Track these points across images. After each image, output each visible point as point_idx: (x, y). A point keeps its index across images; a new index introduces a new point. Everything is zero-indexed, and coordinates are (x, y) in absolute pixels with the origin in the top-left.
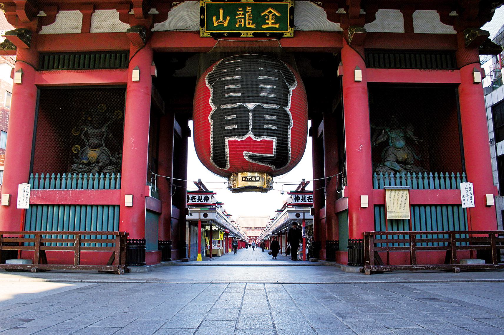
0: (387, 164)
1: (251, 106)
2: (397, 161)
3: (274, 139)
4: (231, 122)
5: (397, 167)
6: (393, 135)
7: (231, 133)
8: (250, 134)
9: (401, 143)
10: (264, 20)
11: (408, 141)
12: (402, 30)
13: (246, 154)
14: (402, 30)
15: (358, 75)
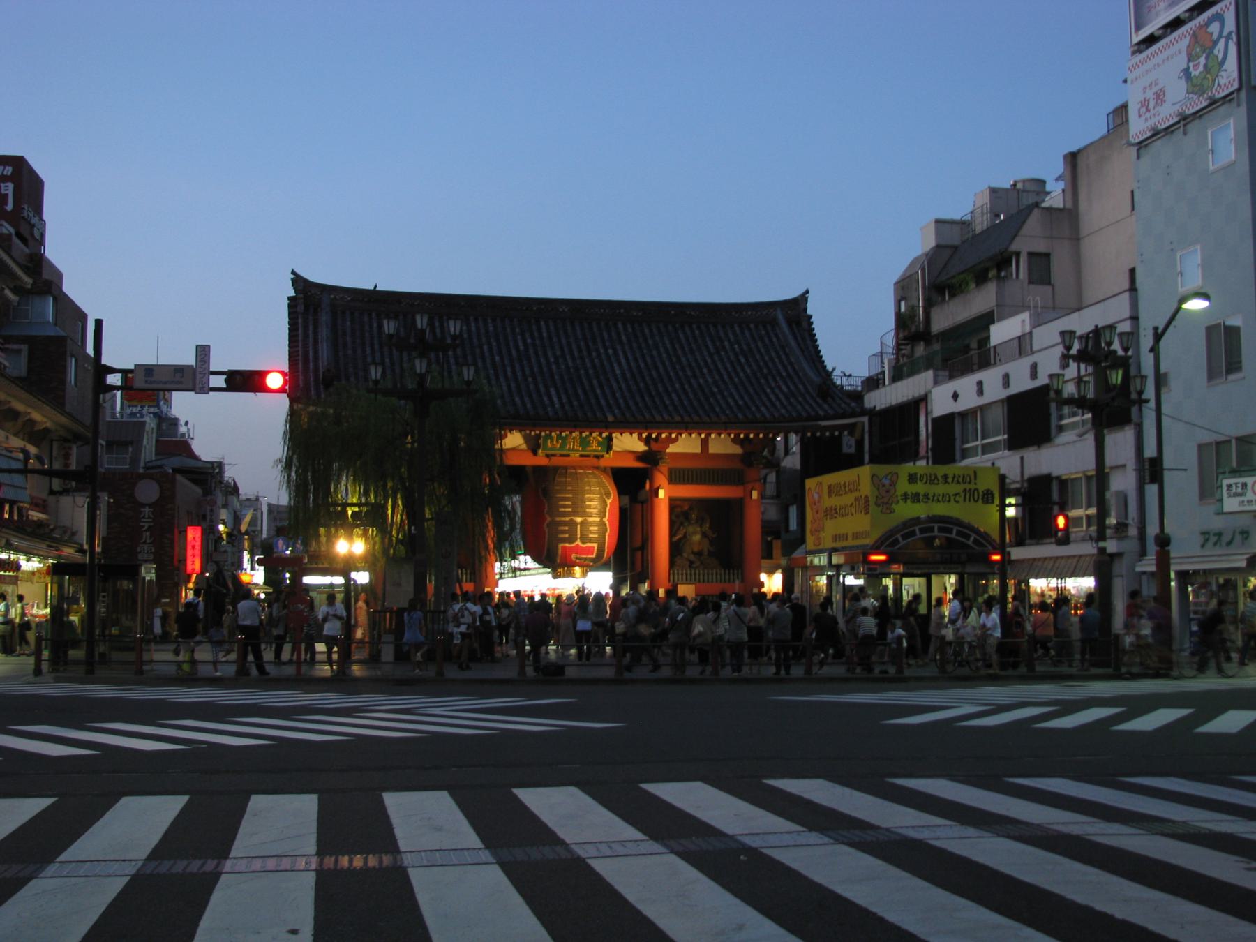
0: (685, 555)
1: (579, 520)
2: (693, 553)
3: (595, 545)
4: (564, 532)
5: (692, 557)
6: (691, 529)
7: (564, 540)
8: (578, 542)
9: (697, 538)
10: (588, 444)
11: (704, 535)
12: (698, 450)
13: (573, 556)
14: (698, 450)
15: (661, 493)
